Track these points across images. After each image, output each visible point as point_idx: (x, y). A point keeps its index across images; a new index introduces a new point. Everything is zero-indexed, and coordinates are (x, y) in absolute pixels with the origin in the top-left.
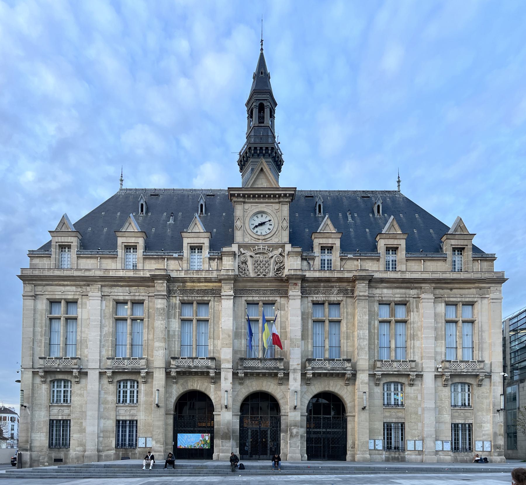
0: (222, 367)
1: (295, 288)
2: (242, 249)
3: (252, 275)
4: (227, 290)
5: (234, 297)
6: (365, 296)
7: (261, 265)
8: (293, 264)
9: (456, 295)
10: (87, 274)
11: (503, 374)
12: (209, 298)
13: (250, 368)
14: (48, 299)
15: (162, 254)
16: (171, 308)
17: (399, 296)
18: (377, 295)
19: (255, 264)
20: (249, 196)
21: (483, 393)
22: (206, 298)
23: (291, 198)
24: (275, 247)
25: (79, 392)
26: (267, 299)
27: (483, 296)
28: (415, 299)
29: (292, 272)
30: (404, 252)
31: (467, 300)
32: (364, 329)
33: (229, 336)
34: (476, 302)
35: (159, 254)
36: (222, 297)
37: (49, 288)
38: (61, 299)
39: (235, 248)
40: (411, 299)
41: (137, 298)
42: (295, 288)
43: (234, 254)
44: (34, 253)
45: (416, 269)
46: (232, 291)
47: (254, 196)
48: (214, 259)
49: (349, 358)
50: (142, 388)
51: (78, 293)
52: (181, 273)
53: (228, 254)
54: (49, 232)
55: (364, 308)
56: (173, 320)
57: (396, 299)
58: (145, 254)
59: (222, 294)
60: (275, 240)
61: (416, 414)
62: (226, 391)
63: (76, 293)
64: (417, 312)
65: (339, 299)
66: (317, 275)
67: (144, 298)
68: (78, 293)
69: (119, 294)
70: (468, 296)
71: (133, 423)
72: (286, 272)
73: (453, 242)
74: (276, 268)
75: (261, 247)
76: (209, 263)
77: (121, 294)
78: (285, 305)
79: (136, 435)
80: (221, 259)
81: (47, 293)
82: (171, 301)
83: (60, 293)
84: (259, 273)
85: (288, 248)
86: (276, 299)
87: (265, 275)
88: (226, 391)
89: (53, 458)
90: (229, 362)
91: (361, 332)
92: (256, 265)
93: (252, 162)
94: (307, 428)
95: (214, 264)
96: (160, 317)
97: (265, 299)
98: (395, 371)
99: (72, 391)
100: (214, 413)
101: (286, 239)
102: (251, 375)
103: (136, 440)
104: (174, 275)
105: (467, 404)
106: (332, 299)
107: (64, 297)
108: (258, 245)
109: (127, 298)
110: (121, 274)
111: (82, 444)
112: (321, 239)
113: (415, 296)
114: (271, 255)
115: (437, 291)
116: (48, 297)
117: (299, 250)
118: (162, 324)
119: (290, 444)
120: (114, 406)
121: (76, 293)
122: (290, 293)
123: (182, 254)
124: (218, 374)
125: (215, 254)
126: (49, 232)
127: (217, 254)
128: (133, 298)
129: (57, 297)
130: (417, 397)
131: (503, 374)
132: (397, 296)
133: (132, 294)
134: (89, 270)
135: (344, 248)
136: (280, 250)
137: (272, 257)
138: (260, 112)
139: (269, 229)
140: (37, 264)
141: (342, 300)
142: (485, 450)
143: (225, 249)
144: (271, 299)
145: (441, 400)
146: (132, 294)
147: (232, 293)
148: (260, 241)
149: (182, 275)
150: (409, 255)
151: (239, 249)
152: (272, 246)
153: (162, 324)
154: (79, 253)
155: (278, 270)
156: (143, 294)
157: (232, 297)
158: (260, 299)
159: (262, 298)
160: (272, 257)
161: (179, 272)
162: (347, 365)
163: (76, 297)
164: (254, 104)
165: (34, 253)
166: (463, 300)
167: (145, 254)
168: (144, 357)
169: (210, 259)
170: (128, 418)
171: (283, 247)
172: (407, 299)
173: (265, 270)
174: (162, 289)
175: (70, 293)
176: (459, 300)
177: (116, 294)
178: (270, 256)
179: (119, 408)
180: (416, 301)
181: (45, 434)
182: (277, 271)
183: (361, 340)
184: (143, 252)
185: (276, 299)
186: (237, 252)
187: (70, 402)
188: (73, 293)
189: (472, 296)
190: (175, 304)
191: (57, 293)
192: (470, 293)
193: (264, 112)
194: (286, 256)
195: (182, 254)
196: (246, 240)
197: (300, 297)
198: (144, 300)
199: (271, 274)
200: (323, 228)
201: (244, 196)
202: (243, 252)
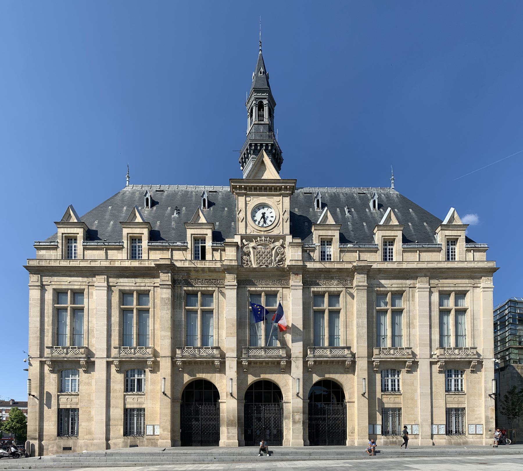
0: (226, 356)
1: (296, 278)
2: (244, 241)
3: (254, 266)
4: (230, 280)
5: (238, 287)
6: (364, 286)
7: (263, 256)
8: (293, 255)
10: (93, 264)
11: (494, 360)
12: (214, 289)
13: (255, 357)
14: (54, 289)
15: (167, 244)
16: (176, 298)
17: (396, 286)
18: (375, 286)
19: (257, 255)
20: (250, 189)
21: (475, 378)
22: (210, 289)
23: (292, 190)
24: (276, 238)
25: (87, 381)
26: (269, 289)
27: (475, 285)
28: (410, 289)
29: (294, 263)
30: (401, 243)
31: (460, 289)
32: (363, 318)
33: (233, 326)
34: (468, 291)
35: (163, 244)
36: (226, 287)
37: (55, 279)
38: (68, 289)
39: (237, 239)
40: (407, 289)
41: (142, 288)
42: (296, 278)
43: (236, 245)
44: (41, 244)
45: (413, 260)
46: (236, 281)
47: (255, 189)
48: (217, 250)
49: (348, 345)
50: (149, 377)
51: (84, 283)
52: (185, 263)
53: (231, 245)
54: (55, 222)
55: (363, 297)
56: (178, 310)
57: (393, 289)
58: (150, 244)
59: (225, 284)
60: (276, 232)
61: (413, 399)
62: (232, 379)
63: (82, 284)
64: (413, 301)
65: (339, 289)
66: (318, 266)
67: (149, 288)
68: (84, 283)
69: (125, 284)
70: (461, 285)
71: (141, 411)
72: (288, 263)
73: (448, 233)
74: (277, 259)
75: (263, 238)
76: (213, 254)
77: (127, 284)
78: (287, 296)
79: (144, 423)
80: (224, 250)
81: (53, 283)
82: (176, 291)
83: (66, 283)
84: (261, 264)
85: (289, 239)
86: (278, 289)
87: (267, 266)
88: (232, 379)
89: (62, 446)
90: (233, 351)
91: (360, 320)
92: (258, 256)
93: (252, 158)
94: (309, 414)
95: (217, 255)
96: (166, 307)
97: (267, 289)
98: (392, 358)
99: (80, 380)
100: (220, 401)
101: (287, 231)
102: (254, 363)
103: (144, 427)
104: (178, 264)
105: (460, 389)
106: (332, 289)
107: (70, 287)
108: (260, 236)
109: (133, 288)
110: (127, 264)
111: (89, 433)
112: (319, 231)
113: (411, 286)
114: (272, 246)
115: (432, 281)
116: (54, 287)
117: (299, 241)
118: (167, 314)
119: (293, 430)
120: (122, 394)
121: (82, 284)
122: (291, 283)
123: (185, 244)
124: (223, 363)
125: (218, 245)
126: (55, 222)
127: (219, 245)
128: (139, 288)
129: (64, 287)
130: (413, 383)
131: (494, 360)
132: (393, 286)
133: (137, 284)
134: (95, 260)
135: (343, 240)
136: (281, 241)
137: (274, 248)
138: (259, 110)
139: (271, 221)
140: (44, 255)
141: (342, 291)
142: (478, 433)
143: (227, 240)
144: (273, 289)
145: (436, 386)
146: (137, 284)
147: (235, 283)
148: (262, 233)
149: (187, 264)
150: (406, 246)
151: (242, 241)
152: (274, 238)
153: (167, 314)
154: (85, 244)
155: (279, 261)
156: (148, 284)
157: (236, 287)
158: (263, 289)
159: (265, 289)
160: (274, 248)
161: (183, 262)
162: (346, 352)
163: (83, 287)
164: (254, 102)
165: (41, 244)
166: (456, 289)
167: (150, 244)
168: (150, 346)
169: (214, 250)
170: (135, 406)
171: (283, 237)
172: (404, 289)
173: (267, 261)
174: (167, 279)
175: (76, 283)
176: (452, 289)
177: (122, 284)
178: (272, 248)
179: (127, 397)
180: (412, 290)
181: (53, 422)
182: (278, 262)
183: (360, 328)
184: (148, 243)
185: (278, 289)
186: (239, 243)
187: (79, 391)
188: (79, 283)
189: (465, 285)
190: (181, 294)
191: (62, 283)
192: (462, 284)
193: (263, 110)
194: (287, 247)
195: (185, 244)
196: (248, 232)
197: (302, 288)
198: (149, 291)
199: (274, 265)
200: (323, 220)
201: (245, 188)
202: (246, 243)
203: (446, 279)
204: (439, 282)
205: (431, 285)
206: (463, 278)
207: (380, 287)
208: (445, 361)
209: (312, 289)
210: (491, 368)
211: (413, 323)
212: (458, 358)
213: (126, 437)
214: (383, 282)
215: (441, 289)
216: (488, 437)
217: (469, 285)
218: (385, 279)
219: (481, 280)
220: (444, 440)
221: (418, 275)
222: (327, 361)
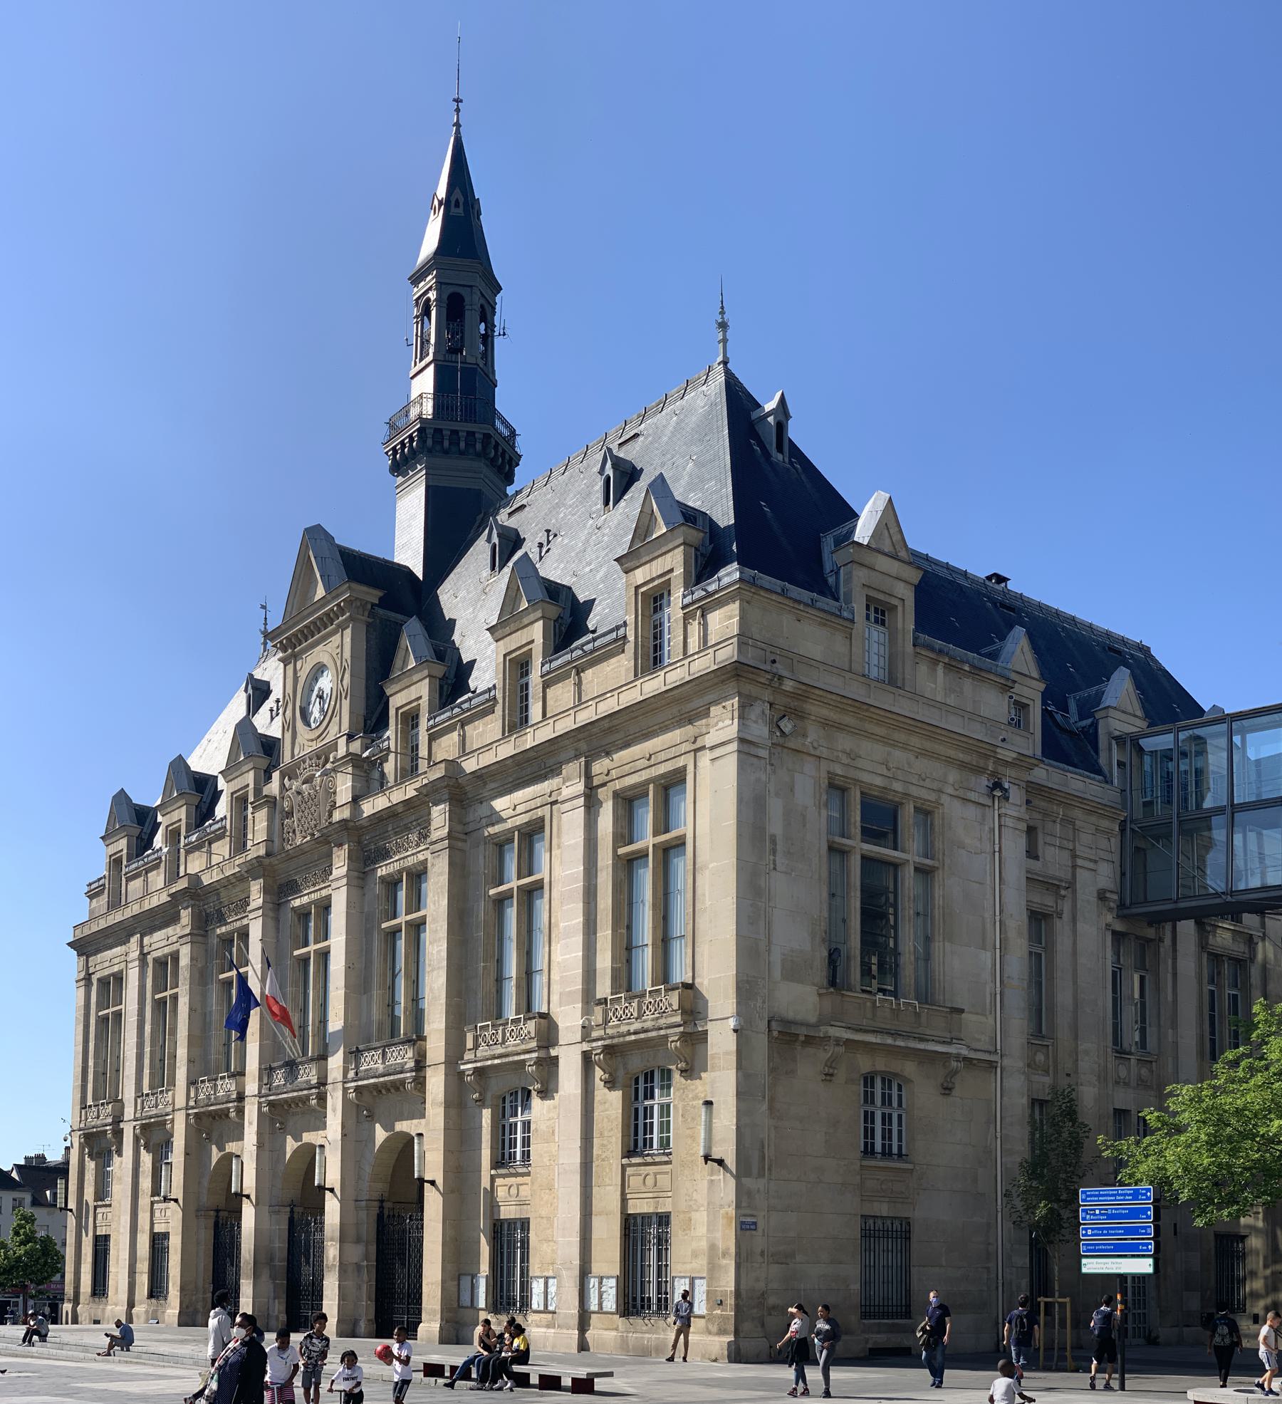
9: (631, 764)
27: (698, 745)
70: (662, 756)
172: (539, 812)
176: (644, 776)
203: (627, 745)
204: (611, 765)
205: (596, 782)
206: (665, 729)
207: (493, 825)
208: (605, 1046)
209: (379, 873)
210: (727, 1053)
211: (557, 926)
212: (629, 1033)
213: (153, 1301)
214: (500, 804)
215: (618, 785)
216: (714, 1329)
217: (685, 747)
218: (501, 795)
219: (711, 721)
220: (614, 1333)
221: (563, 756)
222: (374, 1085)
